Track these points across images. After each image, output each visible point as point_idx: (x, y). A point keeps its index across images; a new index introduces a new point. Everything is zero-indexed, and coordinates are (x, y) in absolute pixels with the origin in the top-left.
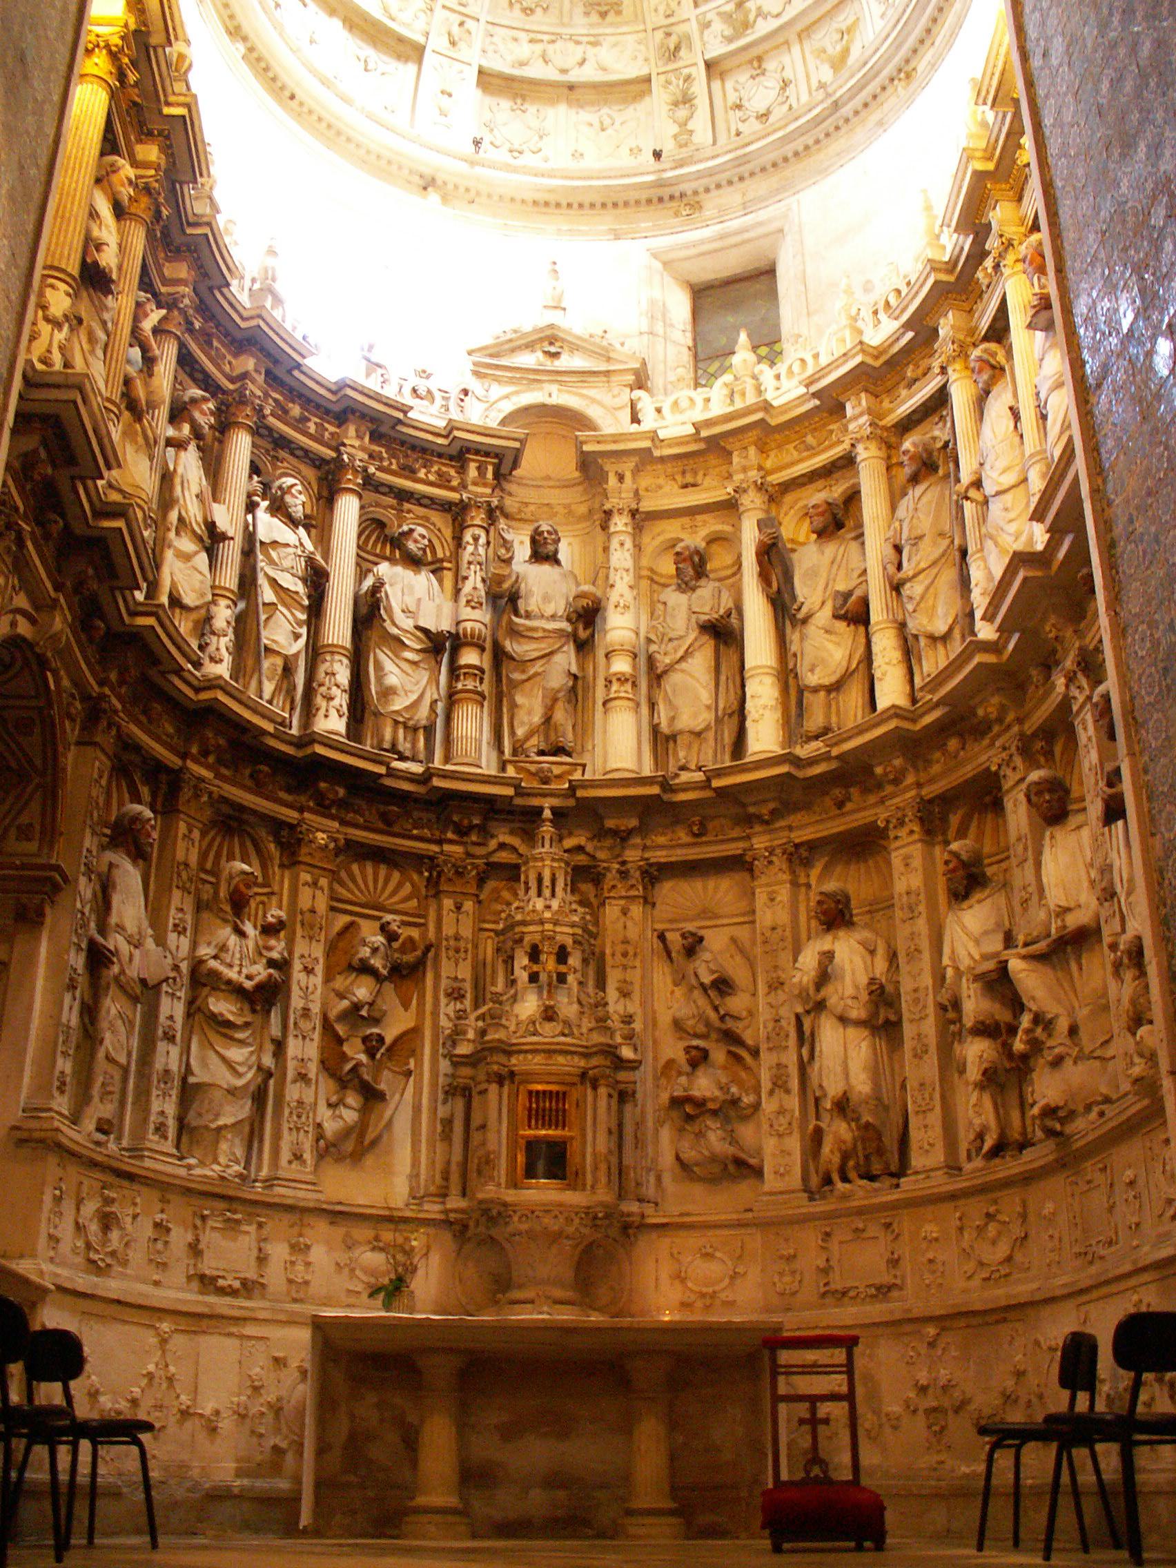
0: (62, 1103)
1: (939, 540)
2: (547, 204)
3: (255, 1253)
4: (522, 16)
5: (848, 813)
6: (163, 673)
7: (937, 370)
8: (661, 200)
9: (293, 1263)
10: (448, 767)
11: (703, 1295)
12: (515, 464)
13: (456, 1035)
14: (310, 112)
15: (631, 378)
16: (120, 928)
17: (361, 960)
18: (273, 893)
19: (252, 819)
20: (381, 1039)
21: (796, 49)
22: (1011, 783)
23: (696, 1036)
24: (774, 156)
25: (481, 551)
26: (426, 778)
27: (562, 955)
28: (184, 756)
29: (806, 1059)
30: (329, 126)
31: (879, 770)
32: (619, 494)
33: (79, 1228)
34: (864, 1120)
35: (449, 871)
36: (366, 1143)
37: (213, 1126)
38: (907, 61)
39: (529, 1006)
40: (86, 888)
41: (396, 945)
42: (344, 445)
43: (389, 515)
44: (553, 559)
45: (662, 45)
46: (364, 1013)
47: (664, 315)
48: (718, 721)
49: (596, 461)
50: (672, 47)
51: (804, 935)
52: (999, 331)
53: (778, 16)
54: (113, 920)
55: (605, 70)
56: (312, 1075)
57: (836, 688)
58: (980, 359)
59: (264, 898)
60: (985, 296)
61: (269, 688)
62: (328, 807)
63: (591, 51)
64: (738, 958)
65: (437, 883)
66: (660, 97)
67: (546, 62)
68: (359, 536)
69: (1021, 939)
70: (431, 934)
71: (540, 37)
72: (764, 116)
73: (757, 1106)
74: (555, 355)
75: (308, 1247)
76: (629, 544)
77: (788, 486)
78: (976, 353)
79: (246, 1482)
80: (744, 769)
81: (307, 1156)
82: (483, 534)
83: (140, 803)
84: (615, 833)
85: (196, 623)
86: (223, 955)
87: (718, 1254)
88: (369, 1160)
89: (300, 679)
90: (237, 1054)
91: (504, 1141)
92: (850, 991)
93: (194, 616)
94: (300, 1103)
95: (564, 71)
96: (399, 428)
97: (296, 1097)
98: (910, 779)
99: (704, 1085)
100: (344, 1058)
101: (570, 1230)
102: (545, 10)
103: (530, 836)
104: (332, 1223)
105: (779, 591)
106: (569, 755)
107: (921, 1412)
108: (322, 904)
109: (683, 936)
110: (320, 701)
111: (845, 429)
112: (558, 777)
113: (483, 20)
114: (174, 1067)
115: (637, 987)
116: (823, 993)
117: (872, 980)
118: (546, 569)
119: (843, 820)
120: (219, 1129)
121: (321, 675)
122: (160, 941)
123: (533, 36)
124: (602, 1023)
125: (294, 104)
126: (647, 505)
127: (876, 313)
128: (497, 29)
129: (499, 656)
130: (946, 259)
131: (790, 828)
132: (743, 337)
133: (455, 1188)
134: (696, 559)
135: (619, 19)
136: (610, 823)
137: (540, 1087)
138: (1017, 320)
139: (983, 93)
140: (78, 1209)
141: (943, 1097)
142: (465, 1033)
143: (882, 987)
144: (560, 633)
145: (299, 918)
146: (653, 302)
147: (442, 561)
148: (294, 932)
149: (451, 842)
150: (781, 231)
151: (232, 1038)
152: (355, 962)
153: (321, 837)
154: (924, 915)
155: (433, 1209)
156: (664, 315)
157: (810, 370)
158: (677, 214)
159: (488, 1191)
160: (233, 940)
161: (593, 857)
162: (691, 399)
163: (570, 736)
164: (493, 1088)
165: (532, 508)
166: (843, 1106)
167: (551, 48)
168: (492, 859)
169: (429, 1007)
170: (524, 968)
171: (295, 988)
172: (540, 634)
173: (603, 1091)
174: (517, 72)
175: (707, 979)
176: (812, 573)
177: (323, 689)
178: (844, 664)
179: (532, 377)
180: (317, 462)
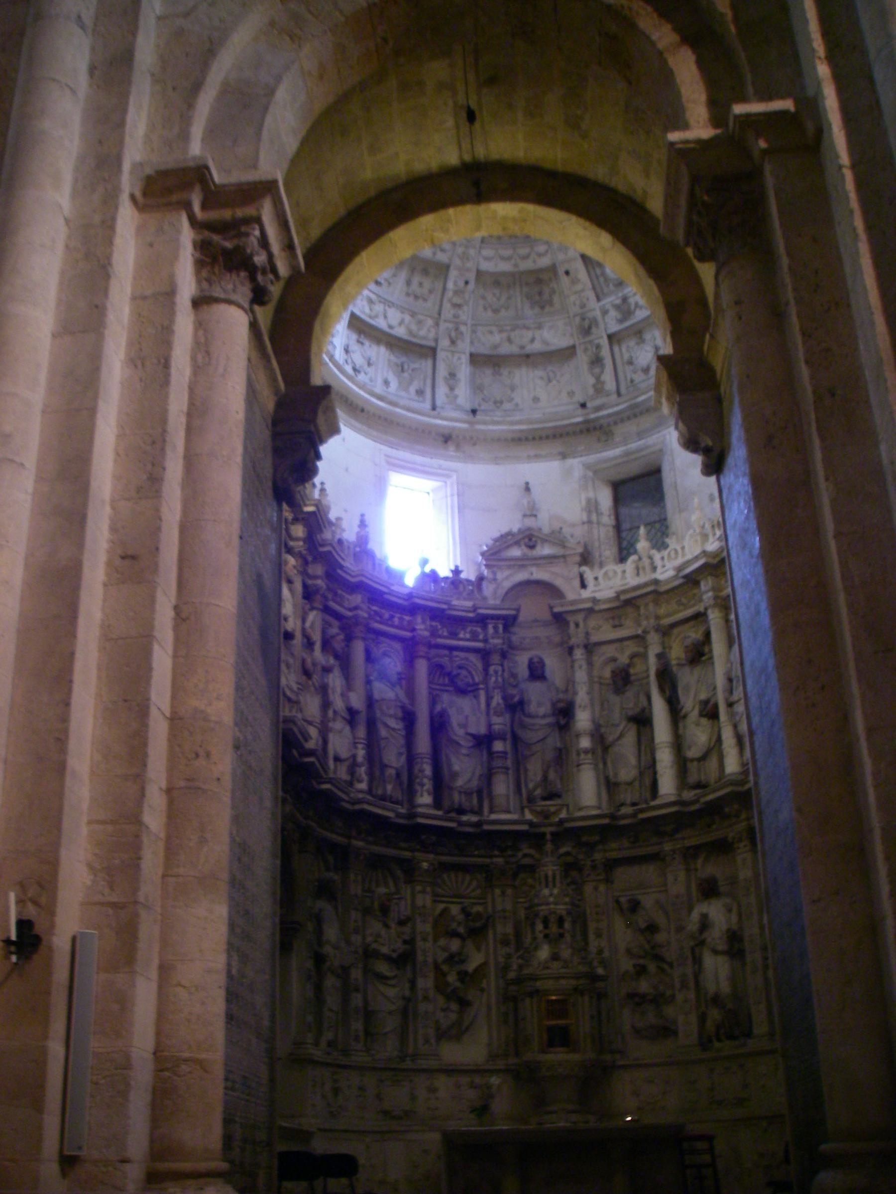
0: (310, 1038)
10: (494, 817)
13: (506, 968)
15: (577, 559)
23: (640, 957)
25: (500, 679)
26: (479, 824)
27: (561, 921)
31: (727, 810)
32: (577, 638)
33: (324, 1097)
39: (544, 953)
40: (310, 926)
41: (470, 918)
43: (445, 661)
48: (641, 774)
50: (586, 326)
63: (537, 334)
66: (582, 359)
70: (490, 909)
73: (673, 996)
74: (532, 547)
76: (585, 667)
82: (499, 668)
90: (391, 992)
93: (346, 764)
95: (522, 347)
98: (743, 816)
99: (644, 986)
110: (418, 788)
117: (728, 930)
120: (386, 1034)
121: (416, 771)
122: (348, 942)
126: (594, 639)
129: (516, 740)
131: (683, 839)
136: (584, 839)
144: (549, 725)
146: (589, 501)
147: (478, 684)
149: (496, 856)
151: (390, 985)
153: (425, 865)
155: (500, 1064)
158: (599, 440)
160: (383, 932)
166: (716, 1000)
167: (512, 334)
169: (491, 951)
170: (540, 932)
175: (643, 925)
177: (418, 780)
179: (521, 563)
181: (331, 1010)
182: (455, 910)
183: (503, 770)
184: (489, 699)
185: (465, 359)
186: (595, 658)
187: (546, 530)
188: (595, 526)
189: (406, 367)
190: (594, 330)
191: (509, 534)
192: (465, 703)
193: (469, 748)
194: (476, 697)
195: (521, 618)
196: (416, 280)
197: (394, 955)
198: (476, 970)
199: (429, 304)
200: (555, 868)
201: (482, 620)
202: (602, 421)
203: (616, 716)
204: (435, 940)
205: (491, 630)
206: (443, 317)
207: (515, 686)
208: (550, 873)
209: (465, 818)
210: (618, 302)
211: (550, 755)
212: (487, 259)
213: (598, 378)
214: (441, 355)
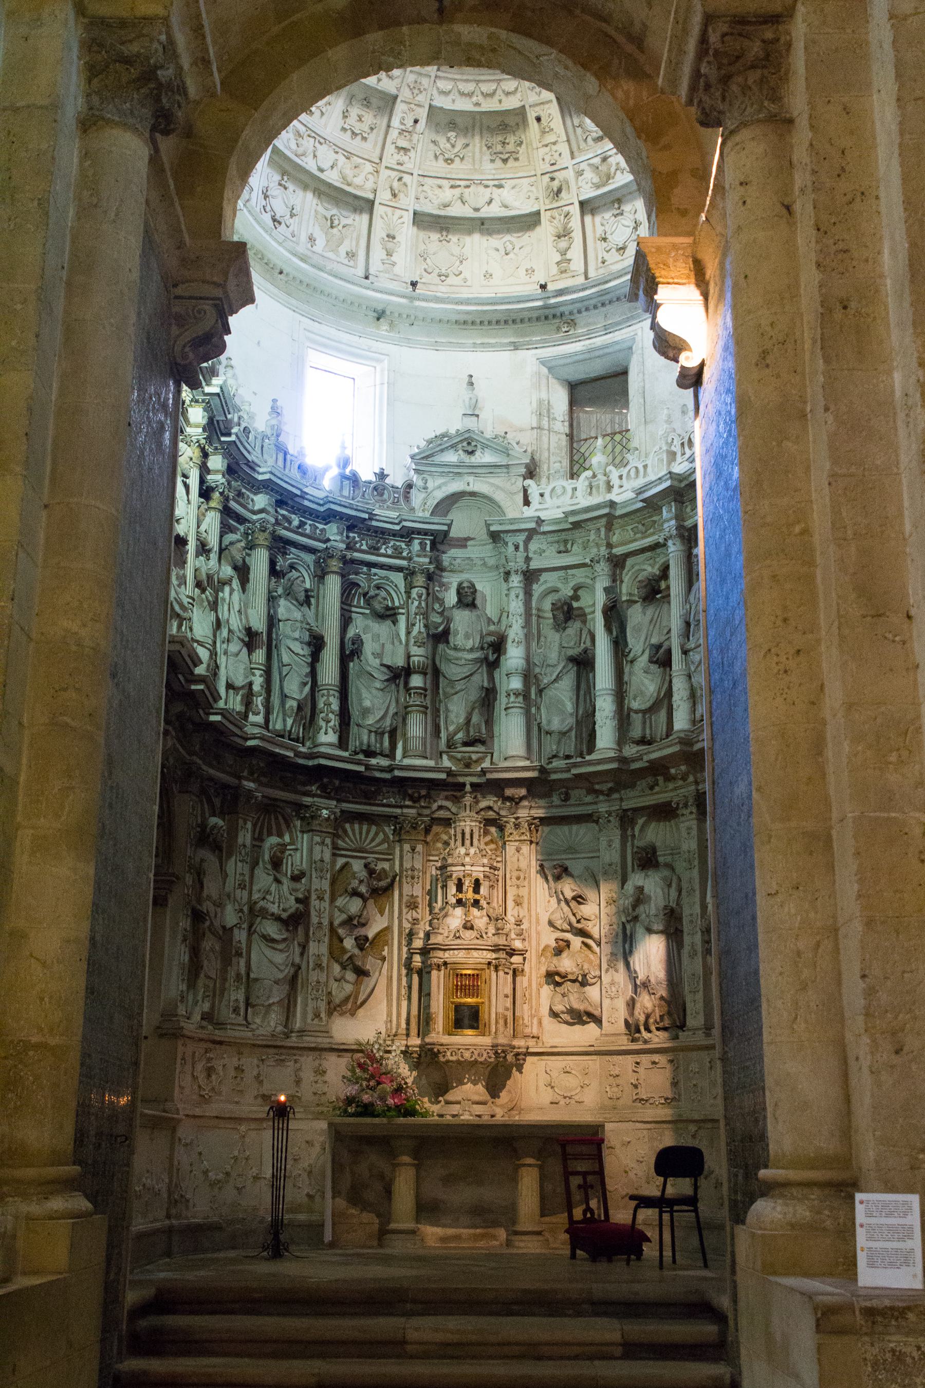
2: (465, 322)
3: (293, 1078)
4: (444, 165)
5: (657, 793)
8: (546, 318)
9: (316, 1082)
10: (407, 762)
11: (565, 1097)
16: (209, 897)
17: (353, 889)
18: (297, 849)
19: (281, 804)
20: (366, 939)
23: (563, 931)
25: (423, 604)
26: (390, 769)
27: (477, 885)
28: (240, 778)
29: (627, 951)
31: (673, 771)
35: (407, 827)
36: (359, 1003)
37: (267, 1003)
39: (456, 919)
42: (328, 540)
44: (472, 605)
45: (548, 187)
47: (548, 411)
49: (499, 536)
50: (555, 189)
51: (630, 868)
55: (506, 207)
56: (324, 965)
61: (290, 721)
62: (329, 793)
65: (400, 834)
66: (546, 229)
67: (464, 204)
68: (342, 595)
71: (458, 183)
74: (472, 453)
75: (325, 1072)
76: (521, 596)
80: (590, 763)
81: (323, 1015)
82: (424, 591)
83: (214, 816)
86: (268, 897)
87: (573, 1072)
88: (361, 1012)
90: (279, 958)
94: (318, 982)
97: (315, 979)
98: (691, 779)
99: (566, 964)
100: (344, 950)
101: (482, 1059)
102: (462, 159)
103: (456, 800)
104: (339, 1056)
105: (617, 637)
108: (327, 856)
110: (323, 724)
112: (476, 762)
113: (415, 174)
114: (243, 971)
115: (526, 901)
117: (665, 907)
119: (652, 798)
120: (270, 1005)
121: (321, 705)
123: (453, 183)
126: (534, 565)
134: (566, 608)
135: (516, 164)
137: (464, 972)
140: (193, 1067)
142: (418, 934)
144: (475, 660)
145: (314, 866)
146: (540, 402)
147: (398, 608)
151: (276, 949)
152: (350, 890)
153: (325, 813)
154: (697, 868)
156: (548, 411)
161: (498, 814)
162: (564, 487)
163: (484, 731)
166: (646, 985)
167: (467, 190)
168: (434, 816)
170: (454, 896)
172: (463, 662)
173: (501, 973)
174: (442, 213)
176: (638, 629)
177: (322, 715)
178: (655, 694)
179: (456, 471)
180: (312, 550)
182: (357, 866)
183: (422, 709)
185: (408, 217)
186: (535, 586)
187: (489, 434)
188: (546, 432)
189: (336, 222)
190: (563, 194)
192: (383, 629)
193: (387, 680)
194: (395, 622)
195: (453, 534)
196: (355, 111)
197: (284, 915)
198: (378, 935)
200: (473, 824)
201: (407, 534)
202: (562, 309)
203: (553, 656)
204: (333, 899)
206: (384, 163)
208: (467, 831)
209: (373, 761)
210: (597, 161)
211: (474, 695)
213: (564, 253)
214: (378, 210)
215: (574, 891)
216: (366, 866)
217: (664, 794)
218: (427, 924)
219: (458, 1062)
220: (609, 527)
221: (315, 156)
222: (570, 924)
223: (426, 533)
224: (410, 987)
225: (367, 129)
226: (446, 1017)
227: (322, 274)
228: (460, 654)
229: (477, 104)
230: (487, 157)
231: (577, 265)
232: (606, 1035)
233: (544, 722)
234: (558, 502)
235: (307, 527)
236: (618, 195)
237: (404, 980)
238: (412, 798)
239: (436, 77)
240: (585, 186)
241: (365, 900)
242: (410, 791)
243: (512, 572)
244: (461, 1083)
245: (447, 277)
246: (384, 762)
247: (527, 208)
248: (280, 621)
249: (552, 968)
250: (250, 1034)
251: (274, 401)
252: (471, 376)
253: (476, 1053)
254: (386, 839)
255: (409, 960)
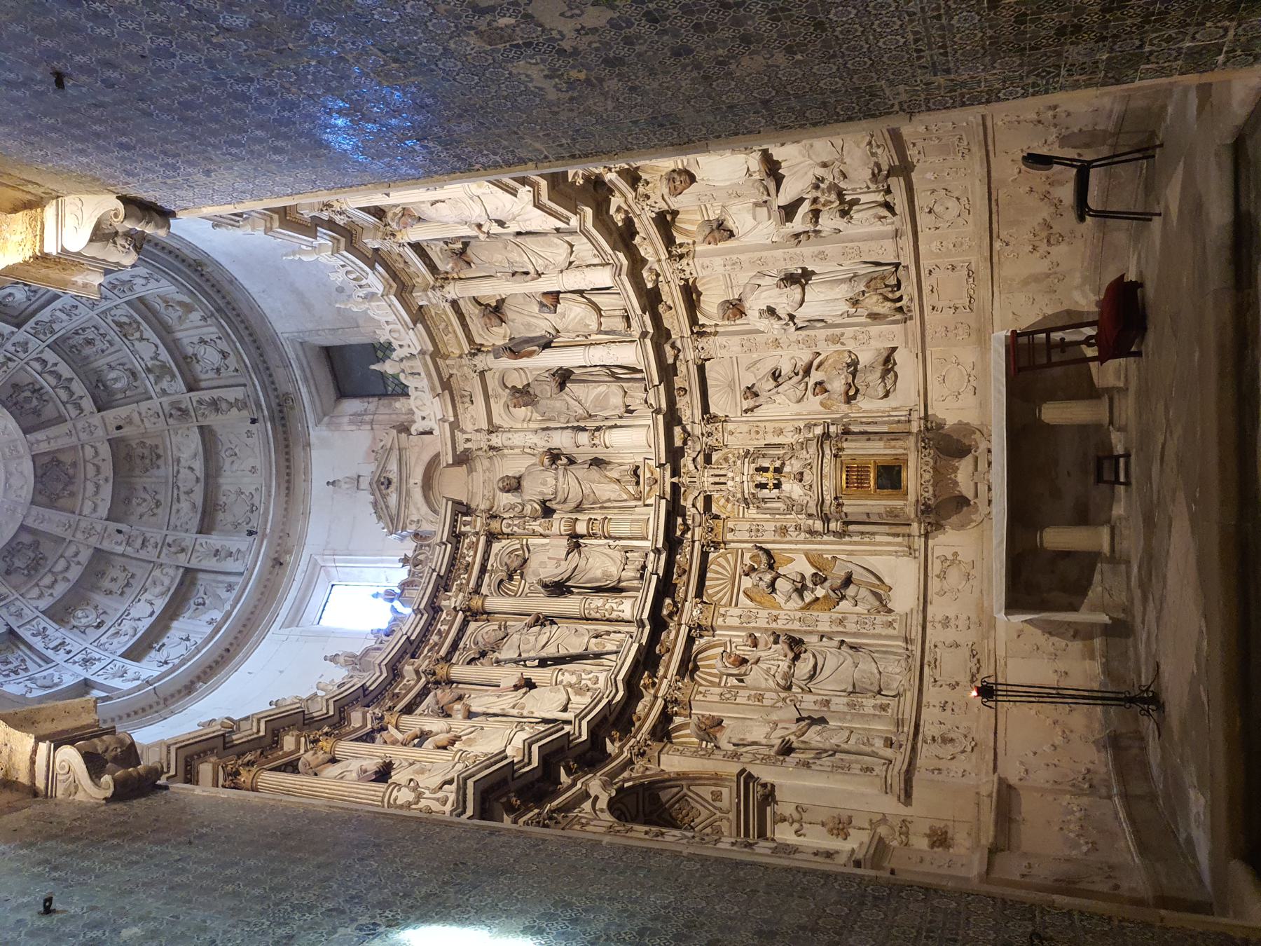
1: (509, 248)
2: (288, 488)
3: (952, 649)
4: (161, 508)
6: (611, 714)
7: (401, 249)
8: (283, 418)
10: (650, 537)
12: (460, 503)
14: (236, 638)
15: (404, 435)
16: (768, 736)
17: (768, 588)
20: (815, 575)
21: (179, 335)
22: (664, 204)
23: (806, 390)
24: (253, 350)
25: (516, 522)
26: (657, 551)
30: (244, 626)
31: (650, 285)
34: (864, 289)
35: (711, 537)
37: (878, 676)
38: (190, 266)
42: (455, 608)
44: (519, 479)
46: (800, 585)
50: (179, 413)
52: (379, 213)
53: (156, 346)
54: (764, 741)
55: (195, 455)
56: (840, 616)
57: (598, 310)
58: (398, 223)
59: (734, 645)
60: (354, 219)
64: (758, 365)
65: (719, 543)
66: (213, 420)
69: (765, 198)
72: (224, 355)
76: (510, 435)
77: (471, 340)
78: (394, 225)
79: (1097, 654)
81: (890, 619)
82: (505, 521)
84: (685, 443)
85: (576, 694)
89: (603, 628)
90: (831, 663)
91: (878, 502)
92: (784, 299)
95: (198, 480)
96: (442, 574)
98: (656, 266)
99: (837, 385)
100: (826, 597)
106: (638, 467)
107: (1049, 249)
108: (737, 612)
109: (746, 398)
110: (614, 615)
111: (436, 306)
113: (167, 532)
114: (845, 700)
115: (777, 425)
116: (782, 316)
117: (778, 286)
118: (525, 483)
120: (880, 673)
121: (598, 616)
123: (175, 500)
124: (804, 445)
125: (231, 650)
126: (485, 426)
127: (360, 286)
128: (171, 523)
130: (330, 244)
132: (373, 367)
133: (905, 530)
134: (517, 395)
135: (161, 447)
138: (378, 200)
139: (232, 222)
141: (852, 241)
143: (782, 280)
146: (351, 422)
147: (522, 547)
148: (754, 628)
150: (301, 343)
152: (769, 590)
155: (919, 543)
156: (359, 415)
157: (399, 327)
158: (292, 408)
159: (911, 511)
164: (845, 509)
165: (486, 492)
166: (855, 302)
167: (182, 489)
171: (787, 627)
174: (200, 510)
175: (772, 384)
178: (583, 306)
179: (405, 495)
180: (465, 623)
181: (849, 738)
182: (747, 583)
184: (534, 534)
185: (202, 539)
189: (200, 601)
191: (375, 504)
196: (106, 584)
199: (138, 572)
200: (706, 474)
201: (456, 537)
202: (274, 405)
203: (558, 404)
205: (467, 528)
207: (523, 506)
210: (151, 377)
211: (595, 473)
212: (95, 509)
213: (231, 405)
214: (194, 564)
215: (768, 380)
216: (747, 575)
217: (672, 295)
218: (800, 516)
219: (935, 485)
220: (445, 357)
221: (139, 619)
222: (800, 382)
223: (454, 521)
224: (862, 533)
225: (124, 575)
226: (888, 497)
227: (234, 614)
228: (559, 489)
229: (107, 480)
230: (155, 472)
231: (238, 393)
232: (907, 343)
233: (617, 412)
234: (428, 403)
235: (442, 628)
236: (181, 360)
237: (855, 539)
238: (684, 533)
239: (80, 515)
240: (174, 388)
241: (778, 576)
242: (678, 533)
243: (490, 443)
244: (956, 483)
245: (253, 505)
246: (651, 556)
247: (196, 437)
248: (520, 655)
249: (842, 398)
250: (909, 694)
251: (325, 659)
252: (328, 483)
253: (924, 468)
254: (724, 556)
255: (835, 533)
